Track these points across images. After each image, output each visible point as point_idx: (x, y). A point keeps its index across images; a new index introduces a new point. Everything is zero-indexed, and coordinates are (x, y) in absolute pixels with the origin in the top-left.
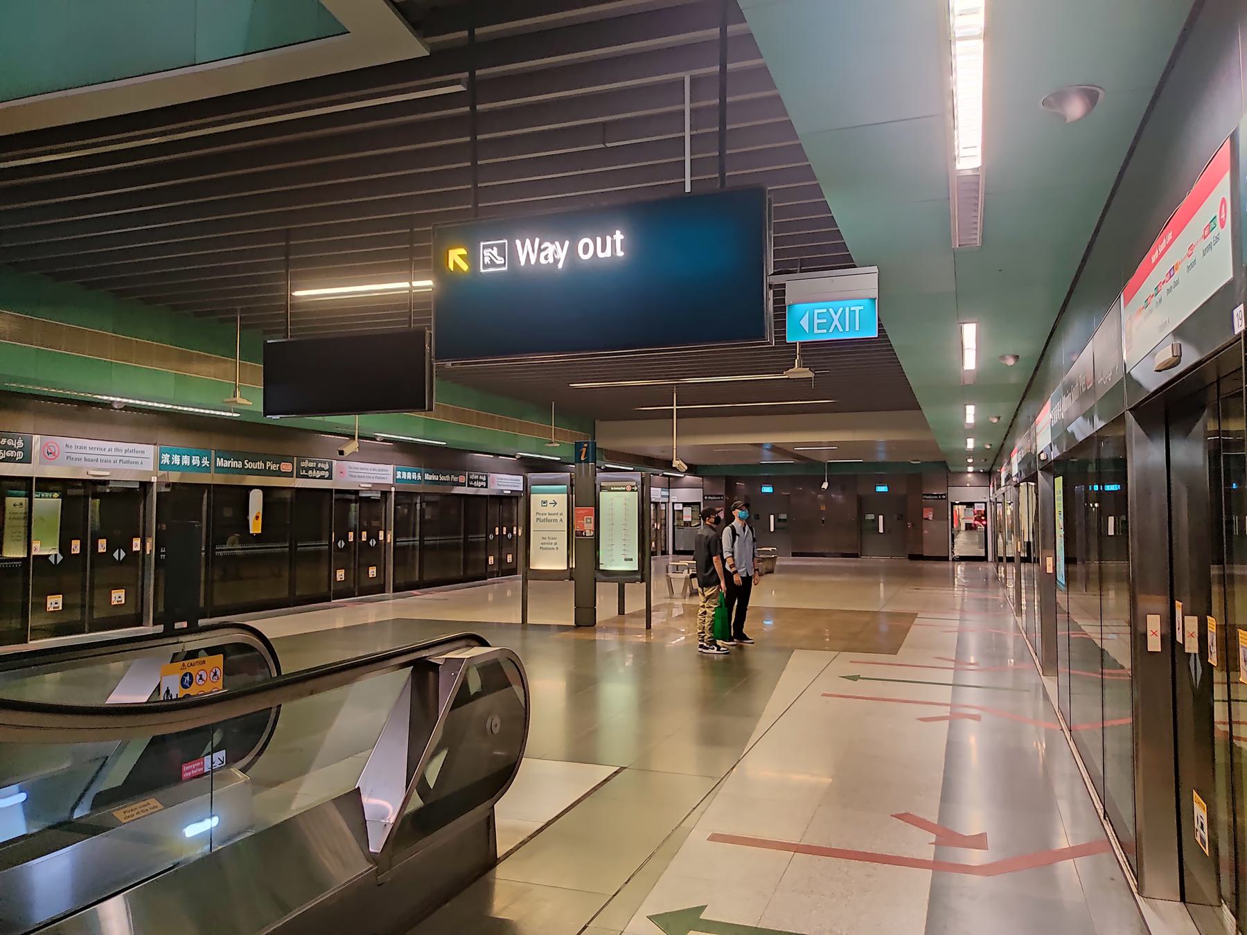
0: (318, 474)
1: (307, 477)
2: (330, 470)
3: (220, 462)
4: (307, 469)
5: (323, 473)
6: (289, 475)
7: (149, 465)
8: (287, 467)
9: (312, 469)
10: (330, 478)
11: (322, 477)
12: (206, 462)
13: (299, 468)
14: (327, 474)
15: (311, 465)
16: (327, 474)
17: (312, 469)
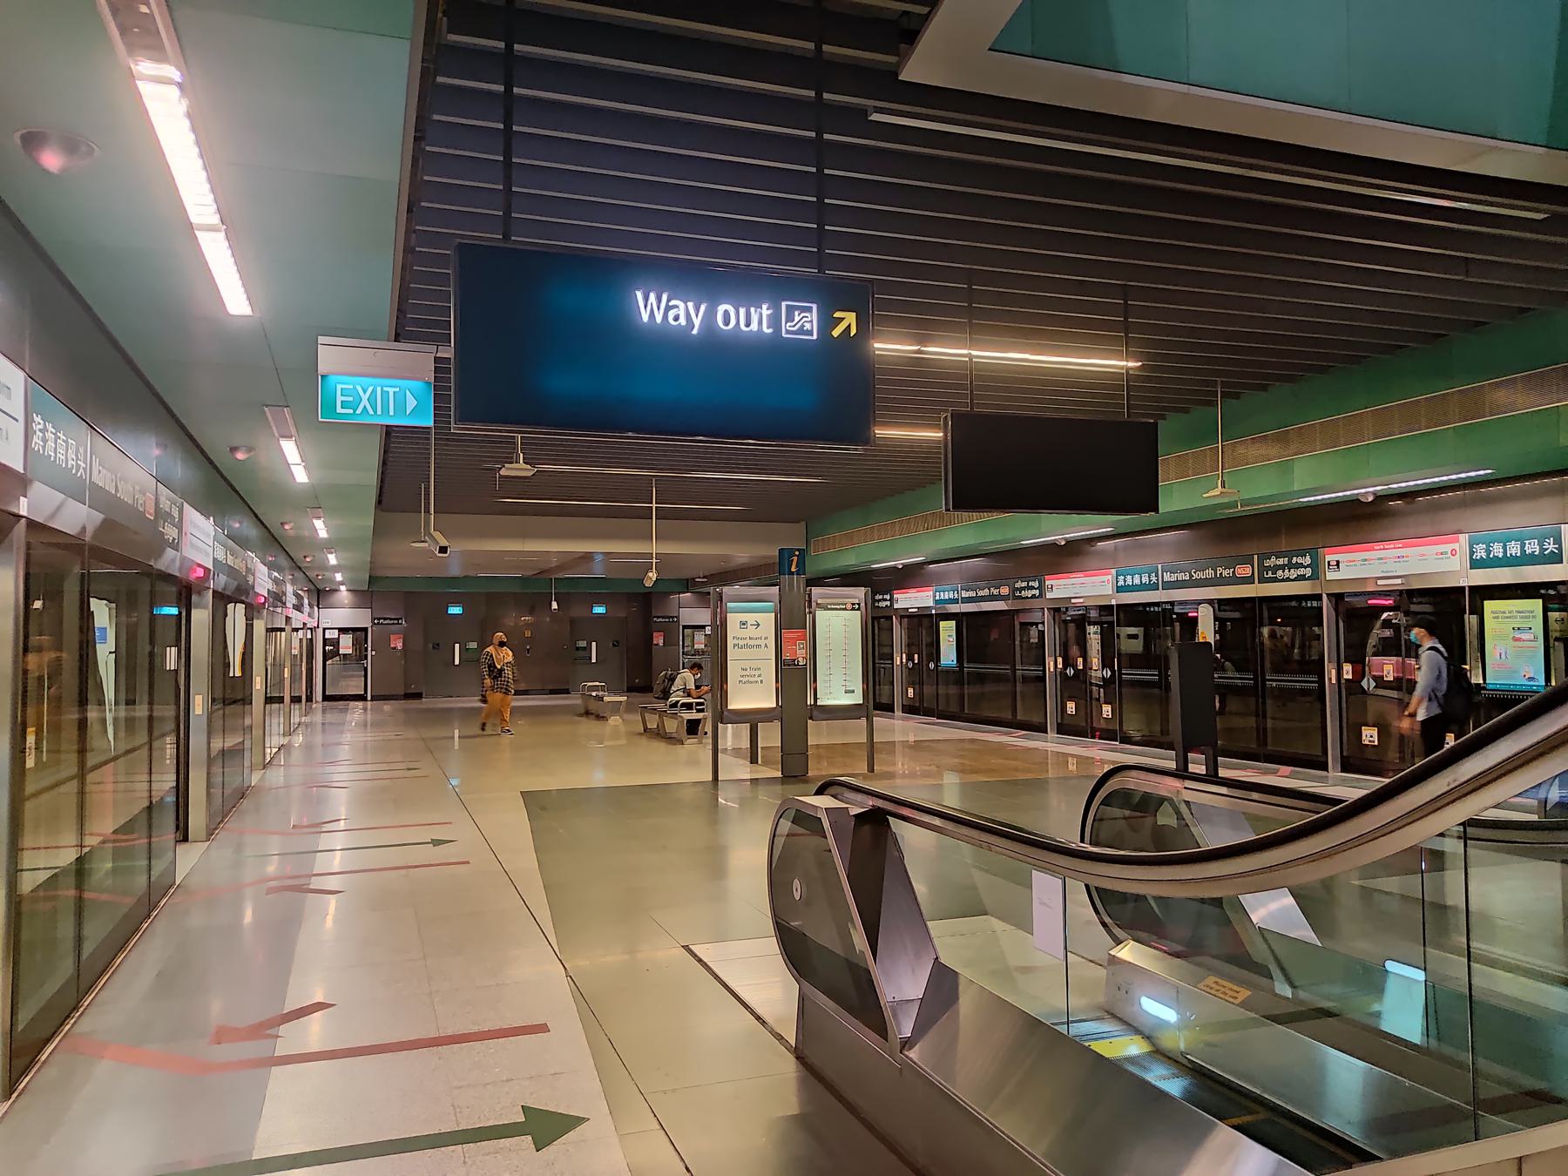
0: (1293, 574)
1: (1275, 580)
2: (1314, 565)
3: (1167, 577)
4: (1276, 568)
5: (1301, 571)
6: (1249, 580)
7: (1108, 589)
8: (1244, 571)
9: (1282, 567)
10: (1315, 577)
11: (1301, 578)
12: (1154, 579)
13: (1263, 569)
14: (1308, 572)
15: (1281, 561)
16: (1308, 572)
17: (1282, 567)
